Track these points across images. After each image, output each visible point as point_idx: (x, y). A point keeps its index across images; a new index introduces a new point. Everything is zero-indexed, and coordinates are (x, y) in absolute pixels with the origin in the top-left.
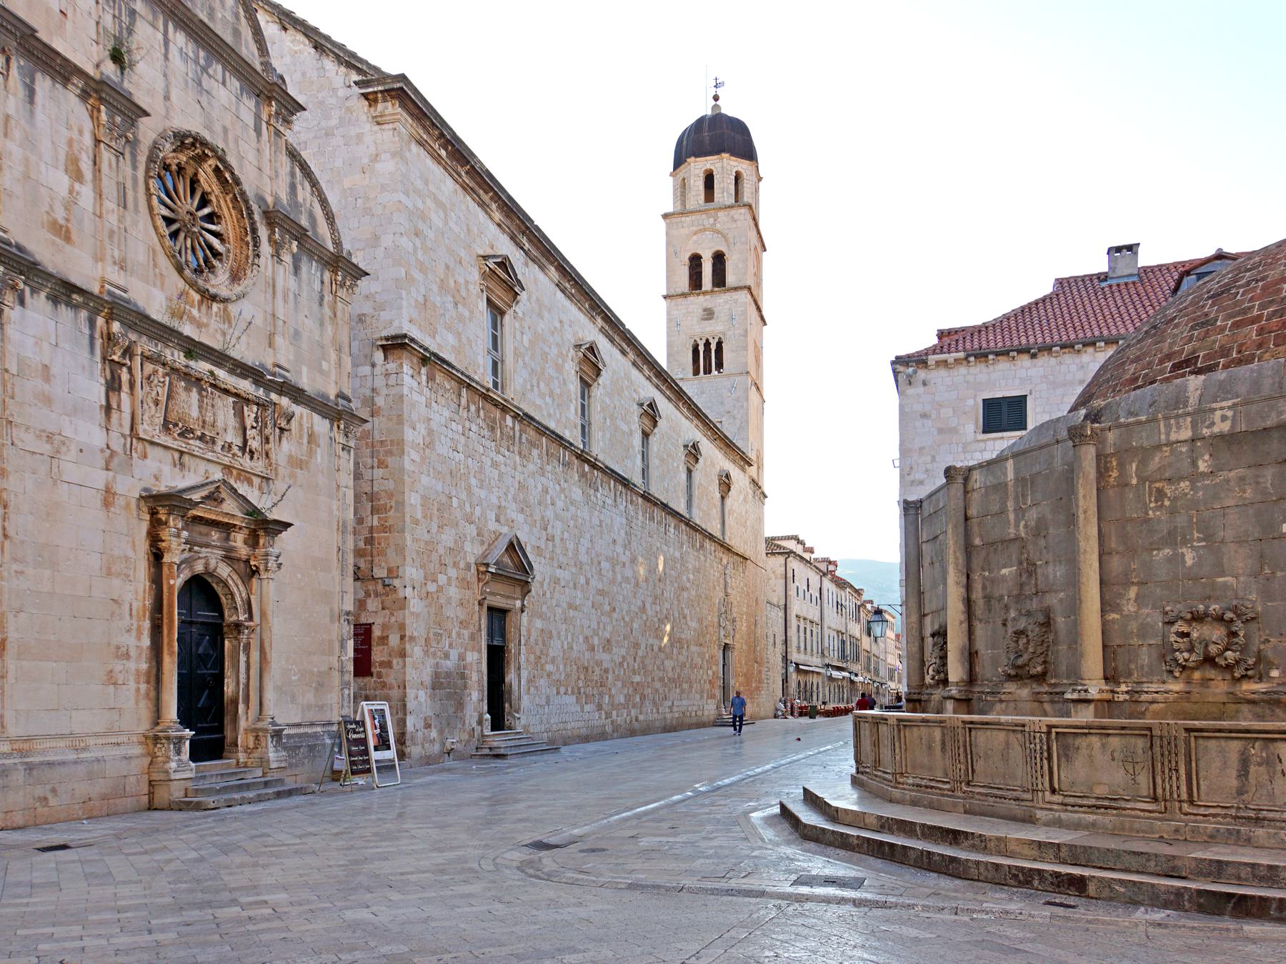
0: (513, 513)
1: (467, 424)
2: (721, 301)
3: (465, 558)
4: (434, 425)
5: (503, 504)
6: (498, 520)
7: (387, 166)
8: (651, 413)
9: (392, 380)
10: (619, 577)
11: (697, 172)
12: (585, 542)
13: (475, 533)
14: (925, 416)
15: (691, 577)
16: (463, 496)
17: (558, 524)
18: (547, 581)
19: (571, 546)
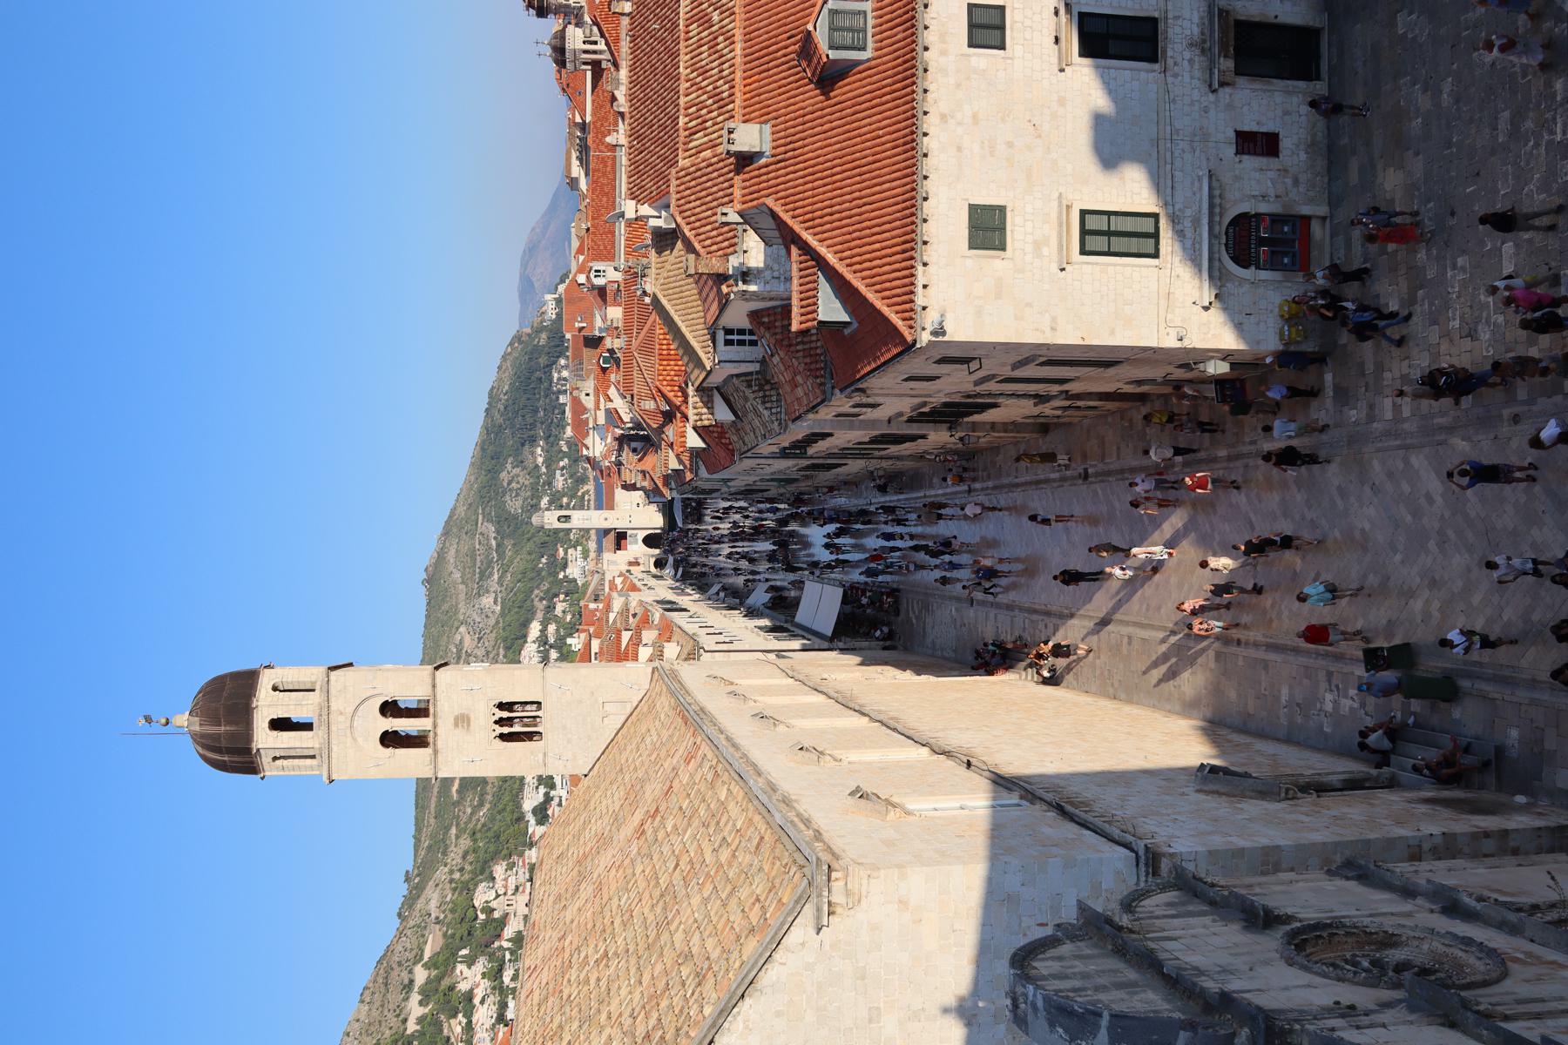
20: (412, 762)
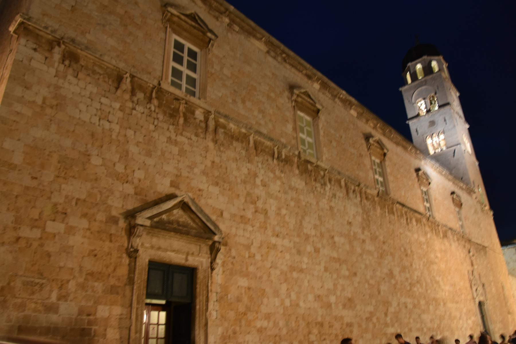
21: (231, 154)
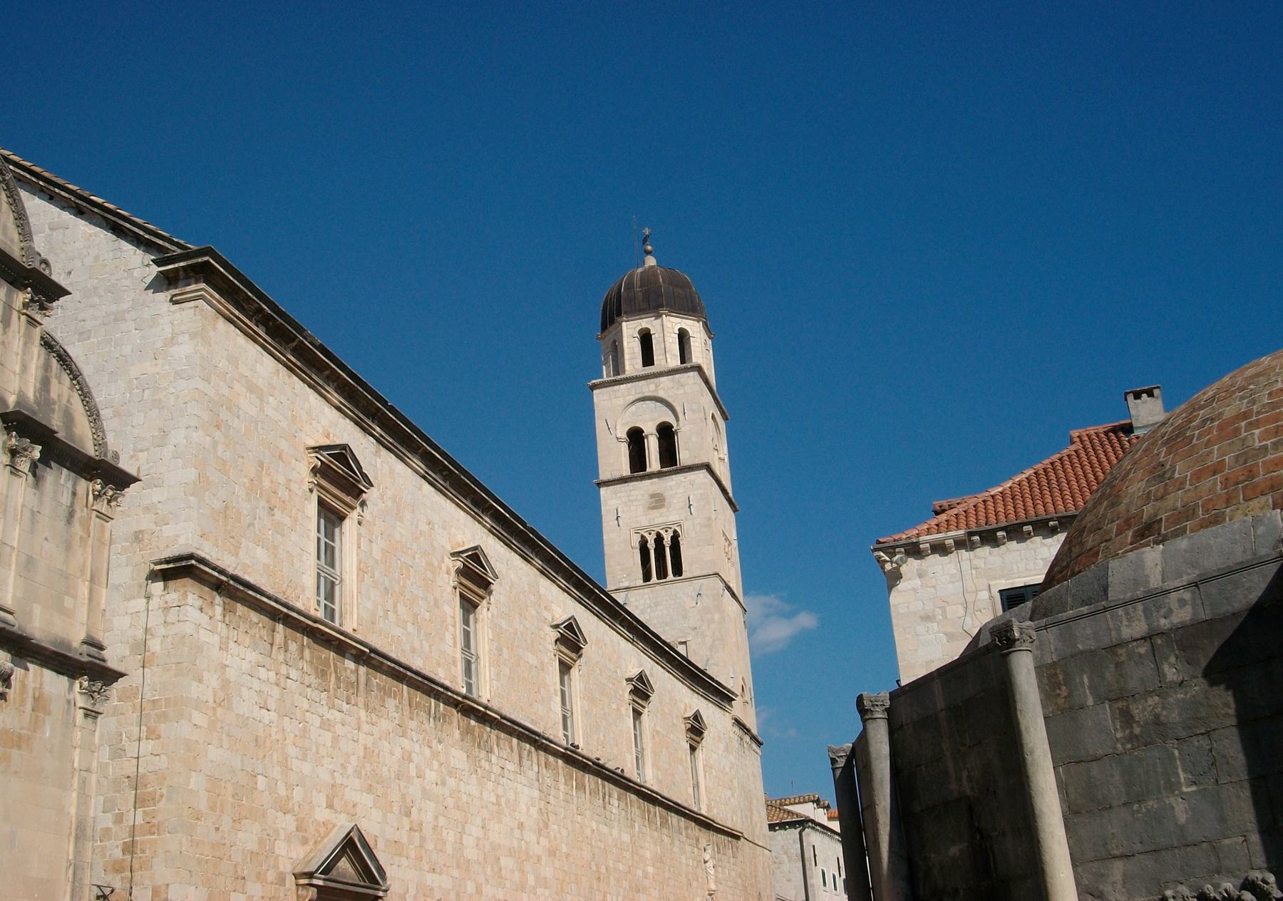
0: (354, 793)
1: (284, 669)
2: (674, 485)
3: (276, 866)
4: (231, 674)
5: (339, 780)
6: (330, 806)
7: (185, 348)
8: (570, 639)
9: (172, 617)
10: (531, 880)
11: (631, 332)
12: (474, 830)
13: (292, 828)
14: (927, 618)
15: (650, 869)
16: (276, 772)
17: (430, 806)
18: (412, 892)
19: (450, 836)
20: (614, 459)
21: (385, 724)
